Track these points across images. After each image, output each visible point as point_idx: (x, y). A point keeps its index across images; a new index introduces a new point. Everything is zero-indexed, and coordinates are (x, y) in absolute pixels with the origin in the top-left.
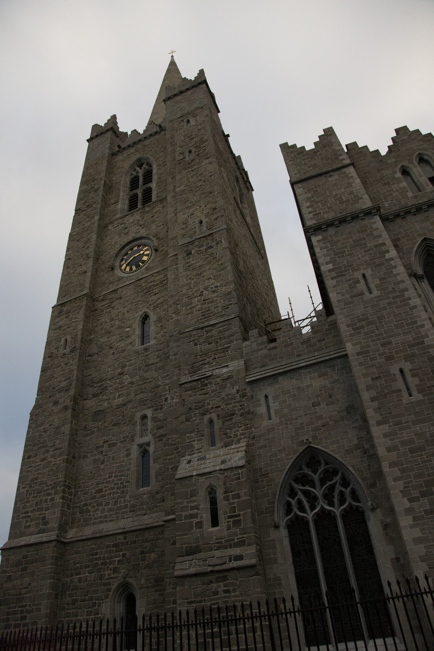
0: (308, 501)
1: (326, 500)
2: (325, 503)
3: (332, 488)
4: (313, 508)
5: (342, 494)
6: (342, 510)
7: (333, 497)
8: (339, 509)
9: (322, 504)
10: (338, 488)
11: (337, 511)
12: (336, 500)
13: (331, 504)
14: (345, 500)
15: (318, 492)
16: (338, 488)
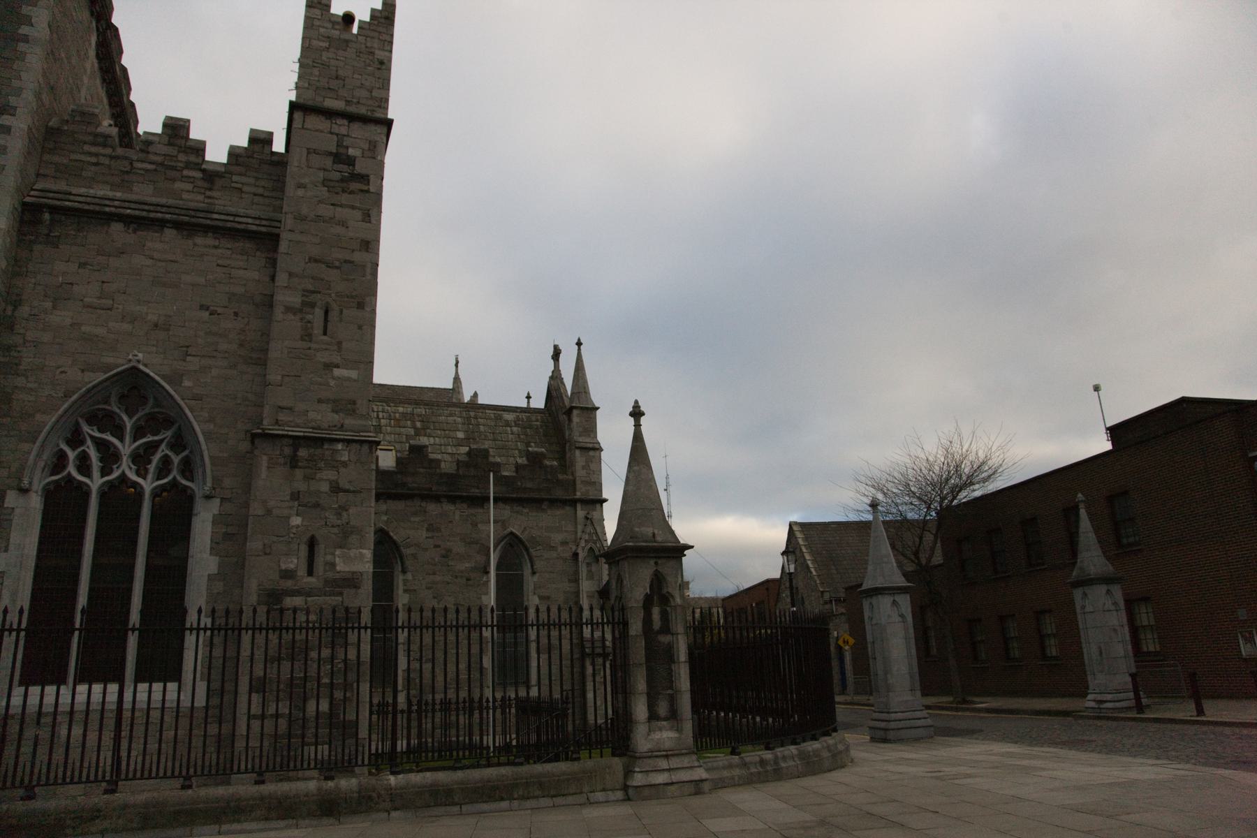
0: (101, 460)
1: (134, 465)
2: (131, 468)
3: (153, 447)
4: (105, 471)
5: (166, 461)
6: (49, 484)
7: (150, 462)
8: (152, 483)
9: (126, 468)
10: (163, 450)
11: (148, 485)
12: (152, 468)
13: (142, 473)
14: (169, 472)
15: (126, 448)
16: (163, 451)
